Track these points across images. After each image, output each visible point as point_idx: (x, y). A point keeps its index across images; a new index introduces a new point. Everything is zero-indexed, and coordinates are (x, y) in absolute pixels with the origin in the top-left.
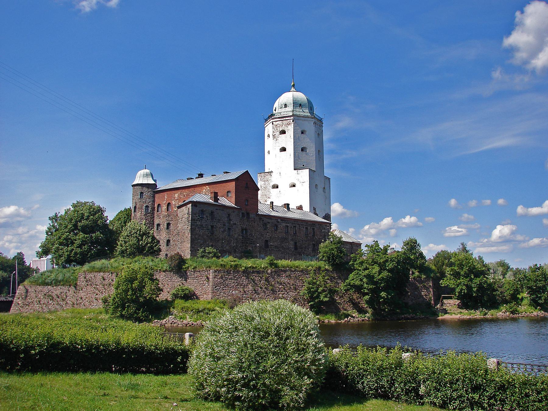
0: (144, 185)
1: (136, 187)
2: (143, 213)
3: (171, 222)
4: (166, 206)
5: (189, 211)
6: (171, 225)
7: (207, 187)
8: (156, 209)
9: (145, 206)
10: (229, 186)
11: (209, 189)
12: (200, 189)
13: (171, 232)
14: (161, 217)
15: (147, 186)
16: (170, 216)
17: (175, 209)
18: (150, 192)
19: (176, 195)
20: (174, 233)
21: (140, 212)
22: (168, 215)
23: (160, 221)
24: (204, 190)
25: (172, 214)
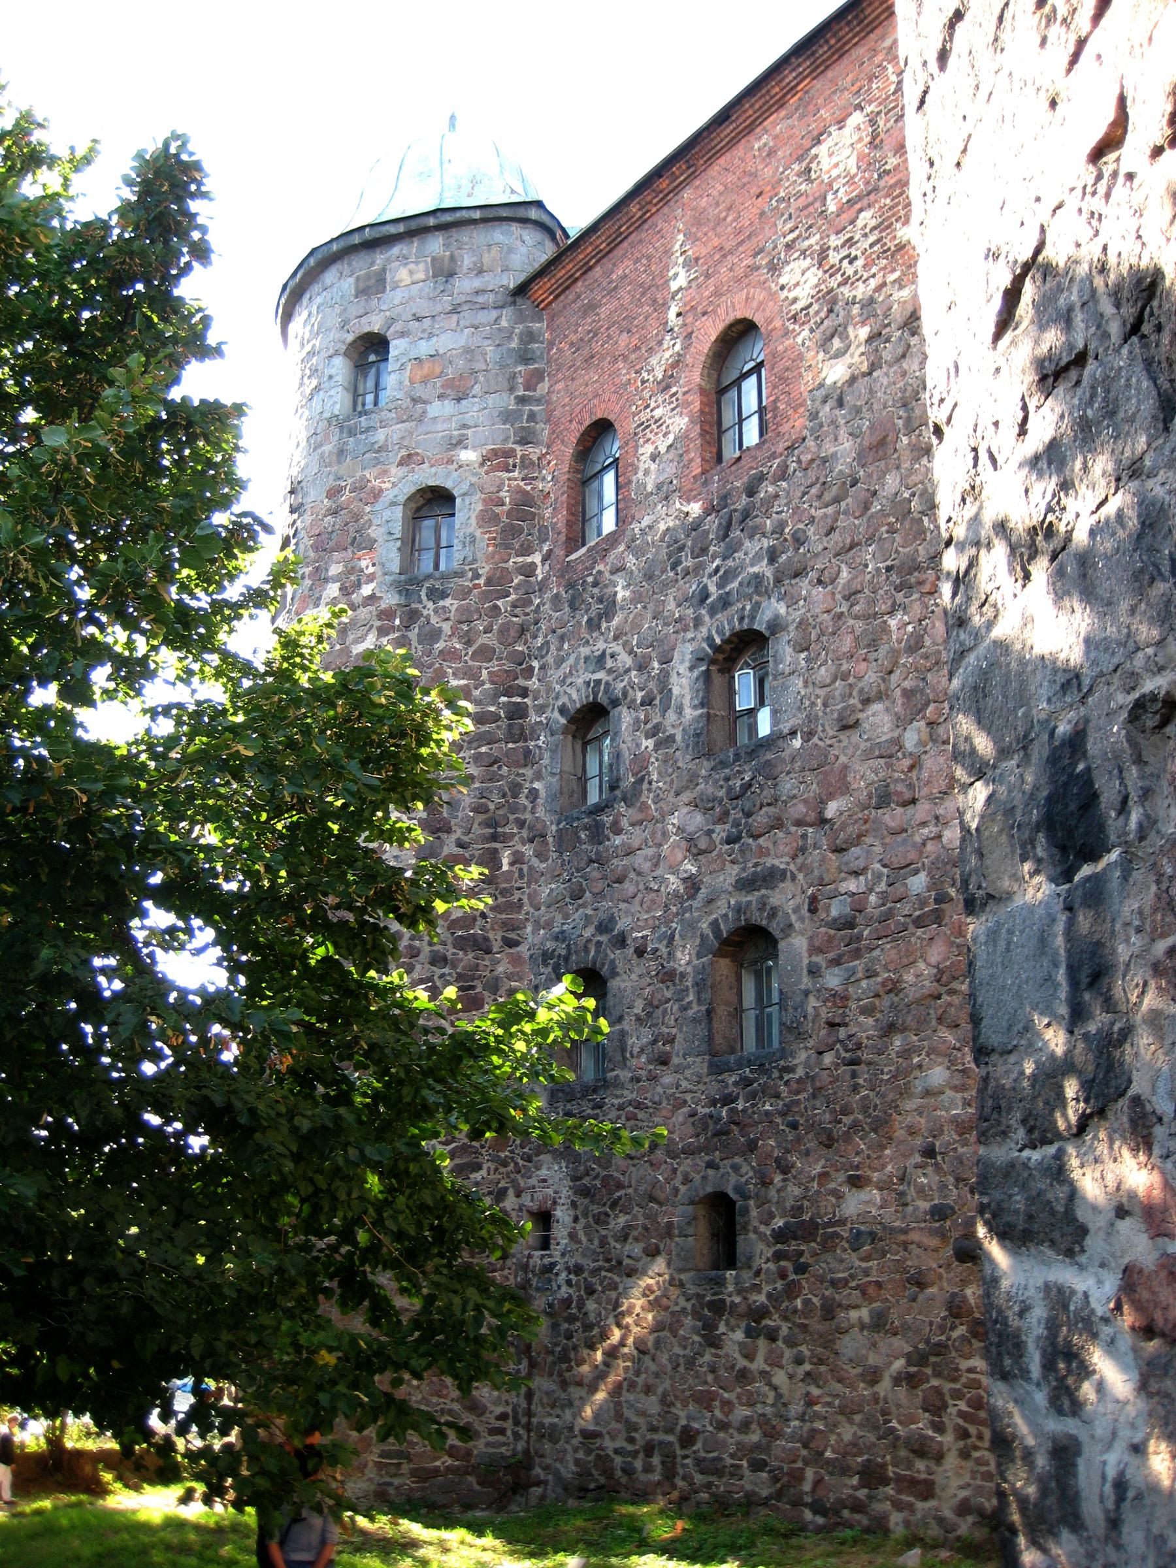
0: (396, 250)
2: (367, 590)
3: (776, 607)
4: (680, 406)
6: (784, 653)
8: (553, 515)
9: (388, 496)
13: (788, 785)
14: (622, 594)
15: (436, 245)
16: (746, 515)
18: (467, 317)
20: (844, 789)
21: (333, 590)
22: (712, 524)
23: (601, 660)
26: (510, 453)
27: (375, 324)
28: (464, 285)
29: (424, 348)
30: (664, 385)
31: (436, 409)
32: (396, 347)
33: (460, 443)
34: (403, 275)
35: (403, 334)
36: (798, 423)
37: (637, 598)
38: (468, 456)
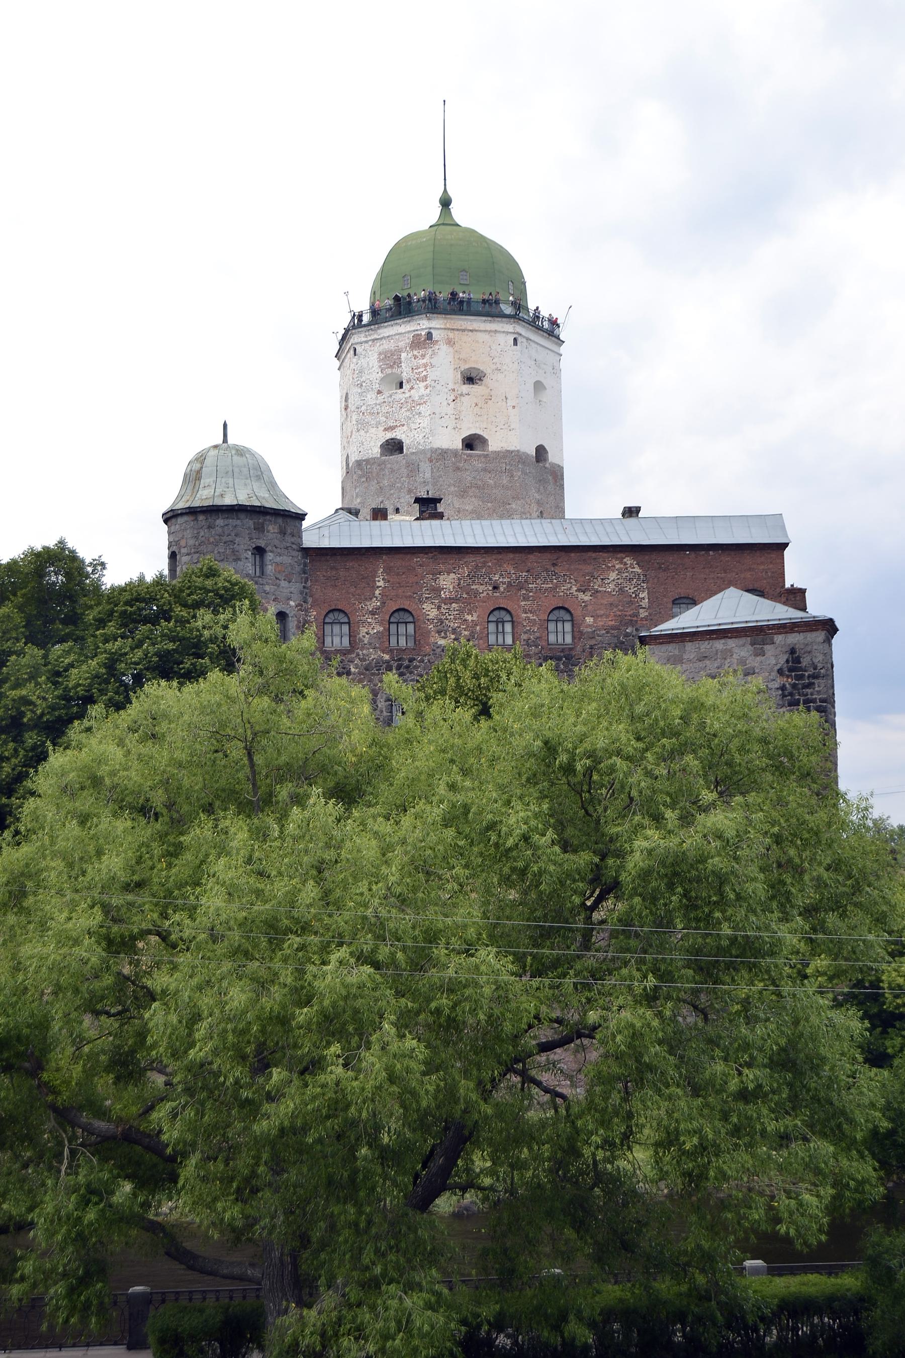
0: (268, 517)
1: (220, 522)
4: (381, 623)
5: (797, 660)
7: (628, 560)
10: (750, 570)
11: (637, 570)
12: (589, 568)
15: (280, 520)
17: (442, 642)
19: (447, 582)
24: (613, 575)
25: (422, 661)
26: (302, 606)
27: (262, 543)
28: (289, 539)
29: (278, 559)
30: (373, 613)
31: (284, 584)
32: (269, 556)
33: (289, 599)
34: (271, 528)
35: (271, 552)
36: (427, 649)
37: (360, 673)
38: (292, 603)
